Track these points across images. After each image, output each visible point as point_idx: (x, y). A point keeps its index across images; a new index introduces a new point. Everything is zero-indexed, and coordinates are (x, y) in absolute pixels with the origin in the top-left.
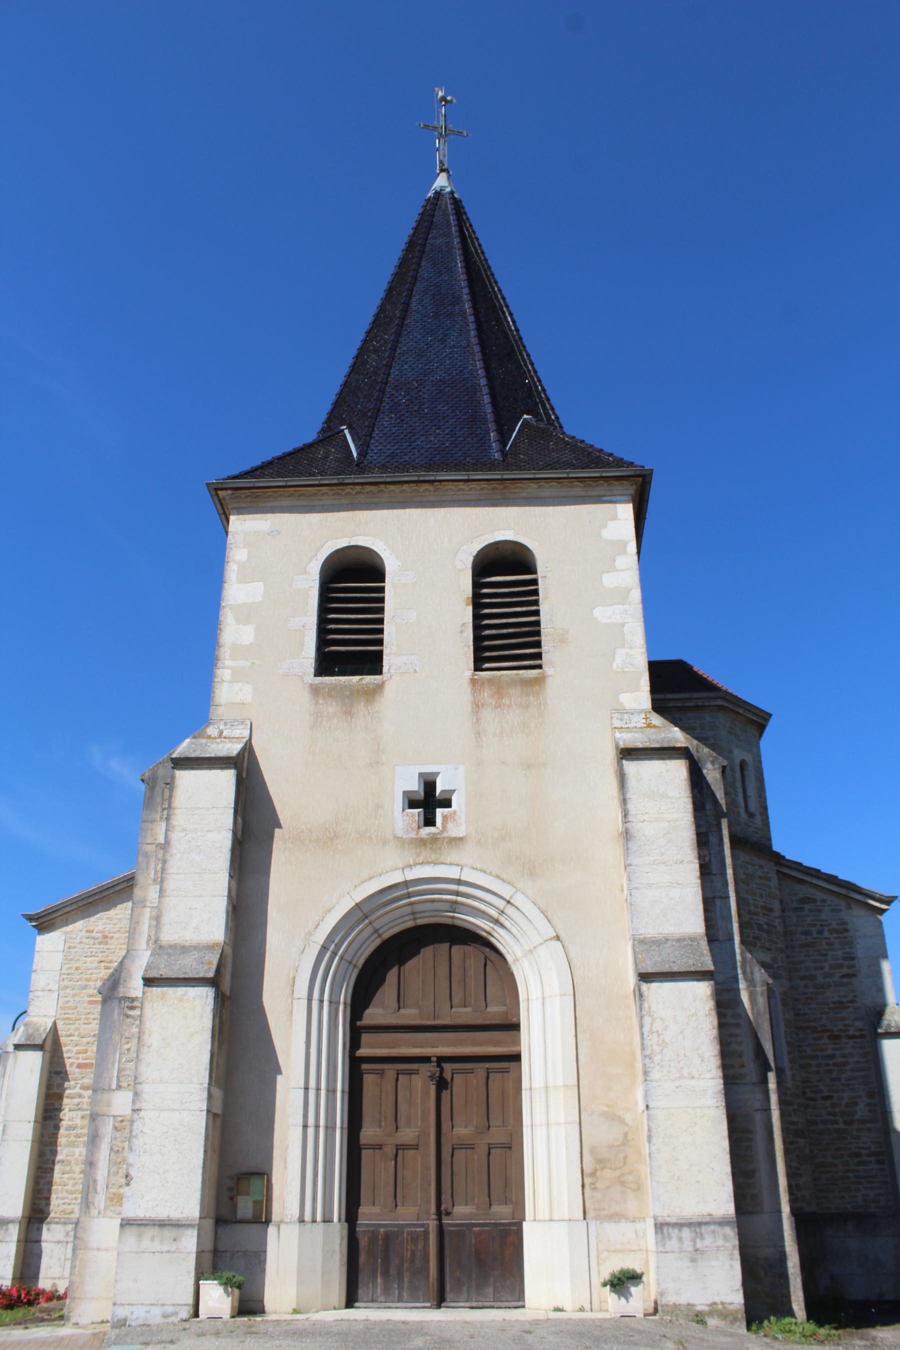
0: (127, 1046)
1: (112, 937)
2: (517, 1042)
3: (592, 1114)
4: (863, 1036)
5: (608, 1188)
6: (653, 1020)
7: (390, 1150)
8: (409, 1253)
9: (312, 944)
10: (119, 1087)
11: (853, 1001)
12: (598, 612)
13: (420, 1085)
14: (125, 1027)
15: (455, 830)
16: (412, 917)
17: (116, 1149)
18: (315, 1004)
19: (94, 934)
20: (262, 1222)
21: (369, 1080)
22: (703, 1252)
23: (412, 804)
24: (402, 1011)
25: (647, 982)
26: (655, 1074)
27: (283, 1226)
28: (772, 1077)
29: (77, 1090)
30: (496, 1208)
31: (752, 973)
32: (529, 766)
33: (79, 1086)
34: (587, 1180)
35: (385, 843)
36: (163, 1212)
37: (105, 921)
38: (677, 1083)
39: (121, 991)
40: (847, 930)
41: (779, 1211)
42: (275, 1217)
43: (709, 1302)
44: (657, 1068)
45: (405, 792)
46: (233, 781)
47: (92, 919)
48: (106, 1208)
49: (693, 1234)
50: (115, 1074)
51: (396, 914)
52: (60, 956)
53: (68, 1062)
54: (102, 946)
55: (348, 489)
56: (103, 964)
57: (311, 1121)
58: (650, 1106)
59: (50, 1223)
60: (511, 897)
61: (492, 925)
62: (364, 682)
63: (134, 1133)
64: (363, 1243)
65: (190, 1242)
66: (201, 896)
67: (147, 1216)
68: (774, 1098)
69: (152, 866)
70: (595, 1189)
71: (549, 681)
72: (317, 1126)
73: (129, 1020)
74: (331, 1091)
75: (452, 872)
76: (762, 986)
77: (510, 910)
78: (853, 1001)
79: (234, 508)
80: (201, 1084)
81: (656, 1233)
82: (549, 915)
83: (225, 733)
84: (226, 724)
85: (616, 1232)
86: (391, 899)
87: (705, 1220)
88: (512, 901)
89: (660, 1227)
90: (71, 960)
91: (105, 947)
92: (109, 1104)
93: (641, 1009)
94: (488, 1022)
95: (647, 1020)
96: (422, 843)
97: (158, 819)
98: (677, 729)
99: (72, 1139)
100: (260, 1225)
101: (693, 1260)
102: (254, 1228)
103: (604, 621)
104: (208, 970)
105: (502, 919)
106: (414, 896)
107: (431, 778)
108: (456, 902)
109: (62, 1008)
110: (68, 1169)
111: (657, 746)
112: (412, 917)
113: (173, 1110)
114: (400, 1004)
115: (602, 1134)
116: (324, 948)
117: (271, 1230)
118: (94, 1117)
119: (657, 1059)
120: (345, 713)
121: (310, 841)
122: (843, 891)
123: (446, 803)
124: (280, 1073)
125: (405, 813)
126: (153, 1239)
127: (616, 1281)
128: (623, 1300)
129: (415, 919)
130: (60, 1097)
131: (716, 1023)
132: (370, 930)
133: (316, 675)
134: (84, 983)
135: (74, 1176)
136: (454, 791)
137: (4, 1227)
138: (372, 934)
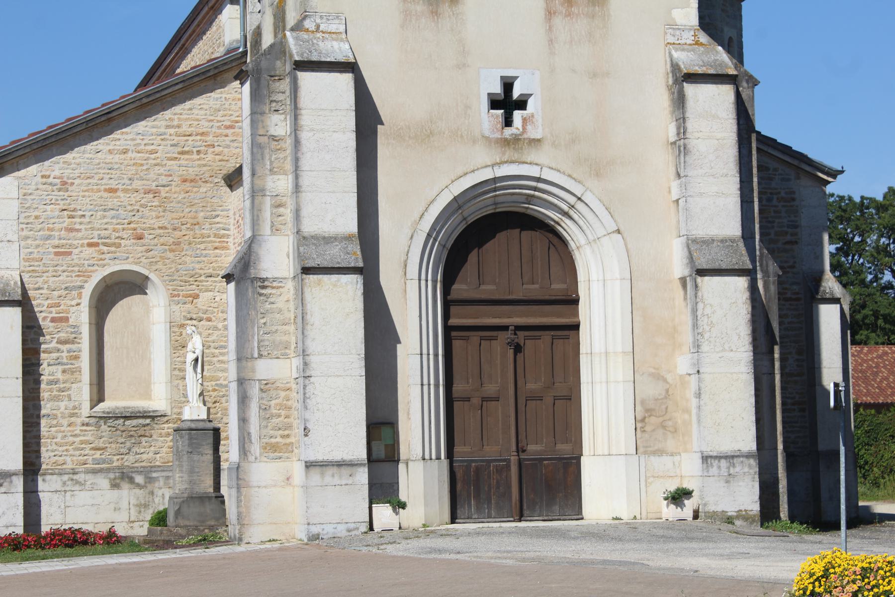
1: (72, 184)
2: (576, 314)
4: (798, 299)
5: (654, 430)
6: (705, 306)
7: (476, 401)
10: (261, 356)
11: (793, 267)
13: (499, 347)
14: (259, 304)
15: (534, 133)
18: (423, 283)
19: (51, 180)
21: (457, 344)
22: (734, 476)
23: (494, 104)
24: (483, 287)
25: (701, 276)
26: (705, 348)
27: (410, 464)
28: (777, 349)
29: (54, 344)
30: (559, 446)
31: (767, 266)
32: (595, 75)
33: (55, 340)
34: (640, 424)
35: (474, 142)
36: (337, 456)
37: (61, 165)
38: (720, 355)
39: (253, 273)
40: (793, 200)
41: (776, 449)
44: (707, 342)
45: (489, 94)
47: (47, 163)
48: (261, 455)
50: (256, 344)
51: (481, 205)
52: (16, 203)
53: (40, 316)
54: (61, 193)
56: (65, 213)
57: (425, 381)
59: (44, 474)
61: (560, 216)
63: (307, 395)
64: (459, 475)
65: (362, 476)
66: (334, 192)
67: (325, 459)
68: (777, 365)
69: (267, 157)
72: (429, 385)
73: (262, 298)
74: (436, 355)
75: (534, 172)
77: (580, 206)
78: (793, 267)
83: (322, 27)
84: (321, 17)
89: (706, 459)
90: (29, 208)
91: (66, 194)
94: (554, 298)
95: (700, 306)
96: (506, 143)
97: (267, 111)
98: (720, 48)
99: (55, 393)
101: (727, 482)
102: (387, 466)
105: (572, 213)
106: (499, 190)
107: (510, 81)
108: (533, 196)
109: (27, 260)
110: (55, 422)
111: (711, 71)
114: (481, 280)
115: (651, 390)
116: (429, 235)
117: (401, 467)
118: (241, 382)
119: (706, 336)
120: (432, 13)
122: (796, 163)
123: (521, 104)
124: (400, 342)
126: (333, 476)
130: (37, 352)
131: (750, 309)
132: (460, 218)
134: (47, 233)
135: (62, 429)
136: (531, 95)
137: (8, 480)
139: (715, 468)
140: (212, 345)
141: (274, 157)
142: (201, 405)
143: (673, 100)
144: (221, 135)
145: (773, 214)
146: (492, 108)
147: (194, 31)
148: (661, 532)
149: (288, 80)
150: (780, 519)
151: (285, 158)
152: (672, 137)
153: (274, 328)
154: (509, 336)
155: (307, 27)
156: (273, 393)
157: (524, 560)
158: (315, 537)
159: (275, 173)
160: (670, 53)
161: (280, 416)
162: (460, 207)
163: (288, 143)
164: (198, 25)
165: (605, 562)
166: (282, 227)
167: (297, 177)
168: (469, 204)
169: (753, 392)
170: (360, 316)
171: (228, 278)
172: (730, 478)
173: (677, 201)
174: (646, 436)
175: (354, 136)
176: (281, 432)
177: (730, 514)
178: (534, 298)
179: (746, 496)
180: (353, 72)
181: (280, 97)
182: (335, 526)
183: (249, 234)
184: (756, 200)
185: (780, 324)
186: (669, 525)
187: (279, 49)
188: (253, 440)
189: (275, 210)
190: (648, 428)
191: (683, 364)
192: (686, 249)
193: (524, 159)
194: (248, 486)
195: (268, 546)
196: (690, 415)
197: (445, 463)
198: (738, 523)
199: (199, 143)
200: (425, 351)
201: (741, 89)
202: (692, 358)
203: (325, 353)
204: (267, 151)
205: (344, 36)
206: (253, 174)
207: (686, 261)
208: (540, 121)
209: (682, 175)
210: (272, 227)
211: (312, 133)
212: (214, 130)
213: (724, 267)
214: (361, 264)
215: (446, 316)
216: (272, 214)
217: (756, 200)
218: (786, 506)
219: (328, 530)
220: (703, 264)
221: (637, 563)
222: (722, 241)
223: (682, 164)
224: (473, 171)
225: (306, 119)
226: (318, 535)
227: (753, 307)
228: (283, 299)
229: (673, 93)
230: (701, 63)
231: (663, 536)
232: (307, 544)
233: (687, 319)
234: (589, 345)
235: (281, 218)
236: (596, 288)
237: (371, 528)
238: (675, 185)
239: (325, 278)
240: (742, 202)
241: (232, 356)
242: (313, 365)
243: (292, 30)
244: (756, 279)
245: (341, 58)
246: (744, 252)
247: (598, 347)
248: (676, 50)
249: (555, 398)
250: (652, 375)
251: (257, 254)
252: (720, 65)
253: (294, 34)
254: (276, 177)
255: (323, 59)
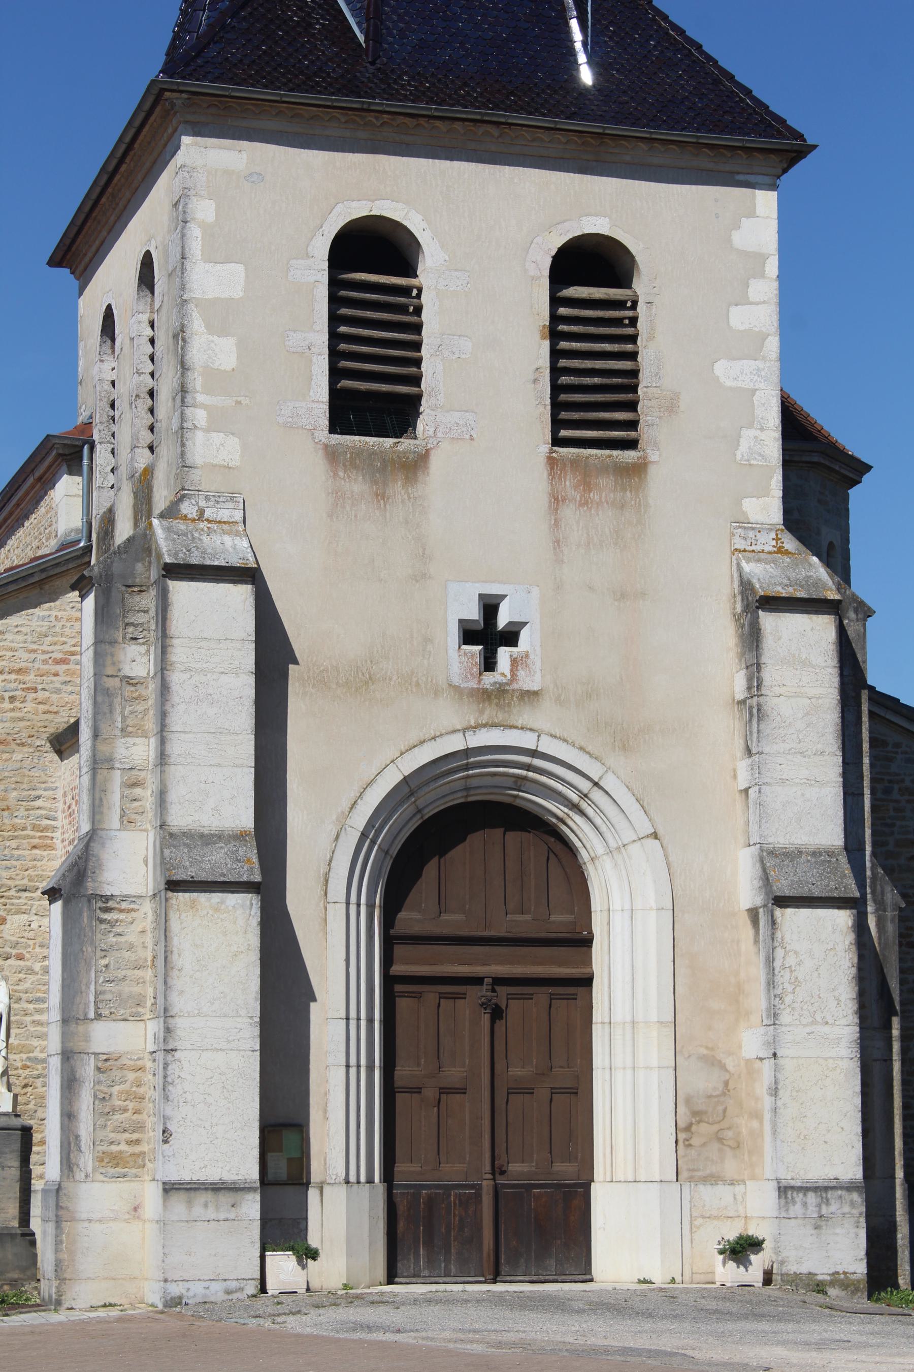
0: (104, 962)
2: (587, 961)
3: (689, 1056)
5: (704, 1145)
7: (430, 1093)
8: (457, 1219)
9: (349, 829)
10: (98, 1016)
12: (720, 368)
13: (467, 1010)
14: (99, 936)
15: (528, 681)
16: (465, 794)
17: (101, 1096)
18: (353, 908)
20: (302, 1184)
21: (403, 1005)
22: (828, 1219)
23: (469, 635)
24: (445, 917)
25: (781, 907)
27: (327, 1189)
28: (896, 1022)
31: (883, 893)
32: (622, 596)
34: (683, 1134)
35: (437, 693)
36: (213, 1175)
38: (808, 1029)
39: (90, 887)
41: (893, 1177)
42: (315, 1177)
43: (830, 1272)
45: (460, 621)
46: (251, 601)
48: (94, 1170)
49: (819, 1199)
50: (92, 999)
55: (371, 118)
57: (353, 1061)
58: (778, 1055)
60: (601, 778)
61: (566, 810)
62: (400, 448)
63: (169, 1079)
64: (402, 1208)
65: (252, 1207)
66: (219, 766)
67: (195, 1178)
68: (896, 1046)
69: (118, 709)
70: (690, 1145)
71: (652, 470)
73: (103, 926)
74: (370, 1021)
75: (527, 741)
76: (894, 910)
77: (596, 795)
79: (186, 122)
80: (251, 1018)
81: (779, 1198)
82: (645, 804)
83: (208, 513)
84: (207, 498)
85: (714, 1196)
86: (445, 771)
87: (831, 1185)
88: (601, 783)
89: (784, 1190)
92: (87, 1039)
93: (773, 939)
94: (554, 935)
95: (779, 953)
96: (485, 696)
97: (120, 639)
98: (815, 559)
100: (297, 1187)
101: (817, 1227)
102: (290, 1190)
103: (729, 383)
104: (251, 869)
105: (584, 805)
106: (473, 768)
107: (494, 602)
108: (525, 778)
112: (465, 794)
113: (217, 1050)
115: (700, 1082)
116: (364, 835)
117: (313, 1194)
118: (67, 1055)
119: (788, 999)
120: (377, 495)
121: (337, 683)
123: (510, 637)
124: (314, 999)
125: (462, 652)
126: (206, 1206)
127: (738, 1248)
128: (742, 1268)
129: (467, 796)
131: (856, 960)
132: (412, 809)
133: (332, 430)
138: (414, 815)
139: (798, 1206)
140: (24, 996)
141: (128, 709)
142: (4, 1090)
143: (741, 636)
144: (48, 673)
145: (892, 813)
146: (465, 643)
147: (11, 514)
148: (713, 1305)
149: (153, 592)
150: (896, 1286)
151: (146, 711)
152: (740, 694)
153: (121, 974)
154: (484, 993)
155: (184, 512)
156: (116, 1074)
157: (499, 1345)
158: (175, 1302)
159: (129, 735)
160: (738, 564)
161: (125, 1110)
162: (412, 793)
163: (151, 690)
164: (18, 505)
165: (625, 1351)
166: (138, 817)
167: (163, 742)
168: (426, 789)
169: (858, 1088)
170: (254, 958)
171: (52, 894)
172: (821, 1222)
173: (746, 791)
174: (693, 1152)
175: (251, 680)
176: (126, 1136)
177: (820, 1278)
178: (524, 935)
179: (844, 1250)
180: (253, 584)
181: (141, 618)
182: (207, 1284)
183: (86, 827)
184: (867, 792)
185: (902, 982)
186: (726, 1294)
187: (142, 544)
188: (83, 1148)
189: (127, 792)
190: (695, 1141)
191: (751, 1042)
192: (758, 865)
193: (512, 722)
194: (73, 1219)
195: (101, 1313)
196: (761, 1123)
197: (380, 1188)
198: (833, 1292)
199: (13, 685)
200: (353, 1014)
201: (846, 622)
202: (766, 1034)
203: (199, 1015)
204: (117, 701)
205: (241, 528)
206: (96, 735)
207: (757, 883)
208: (538, 664)
209: (754, 751)
210: (122, 817)
211: (188, 675)
212: (37, 665)
213: (816, 894)
214: (257, 878)
215: (387, 960)
216: (122, 797)
217: (867, 792)
218: (908, 1267)
219: (195, 1291)
220: (784, 888)
221: (675, 1354)
222: (814, 854)
223: (755, 735)
224: (434, 738)
225: (179, 653)
226: (180, 1298)
227: (861, 957)
228: (137, 928)
229: (743, 626)
230: (785, 581)
231: (716, 1311)
232: (162, 1312)
233: (759, 972)
234: (607, 1009)
235: (136, 804)
236: (619, 922)
237: (263, 1289)
238: (743, 766)
239: (203, 899)
240: (845, 794)
241: (55, 1015)
242: (179, 1032)
243: (162, 516)
244: (866, 913)
245: (235, 561)
246: (848, 871)
247: (621, 1013)
248: (748, 561)
249: (553, 1091)
250: (703, 1058)
251: (98, 859)
252: (815, 585)
253: (165, 523)
254: (131, 740)
255: (208, 562)
